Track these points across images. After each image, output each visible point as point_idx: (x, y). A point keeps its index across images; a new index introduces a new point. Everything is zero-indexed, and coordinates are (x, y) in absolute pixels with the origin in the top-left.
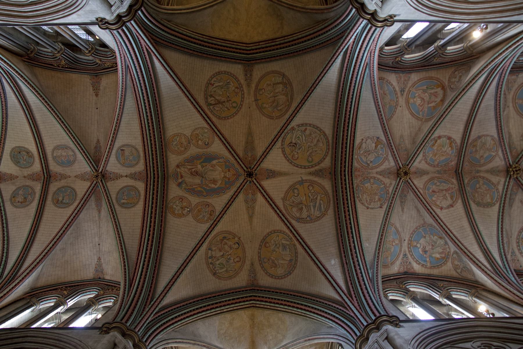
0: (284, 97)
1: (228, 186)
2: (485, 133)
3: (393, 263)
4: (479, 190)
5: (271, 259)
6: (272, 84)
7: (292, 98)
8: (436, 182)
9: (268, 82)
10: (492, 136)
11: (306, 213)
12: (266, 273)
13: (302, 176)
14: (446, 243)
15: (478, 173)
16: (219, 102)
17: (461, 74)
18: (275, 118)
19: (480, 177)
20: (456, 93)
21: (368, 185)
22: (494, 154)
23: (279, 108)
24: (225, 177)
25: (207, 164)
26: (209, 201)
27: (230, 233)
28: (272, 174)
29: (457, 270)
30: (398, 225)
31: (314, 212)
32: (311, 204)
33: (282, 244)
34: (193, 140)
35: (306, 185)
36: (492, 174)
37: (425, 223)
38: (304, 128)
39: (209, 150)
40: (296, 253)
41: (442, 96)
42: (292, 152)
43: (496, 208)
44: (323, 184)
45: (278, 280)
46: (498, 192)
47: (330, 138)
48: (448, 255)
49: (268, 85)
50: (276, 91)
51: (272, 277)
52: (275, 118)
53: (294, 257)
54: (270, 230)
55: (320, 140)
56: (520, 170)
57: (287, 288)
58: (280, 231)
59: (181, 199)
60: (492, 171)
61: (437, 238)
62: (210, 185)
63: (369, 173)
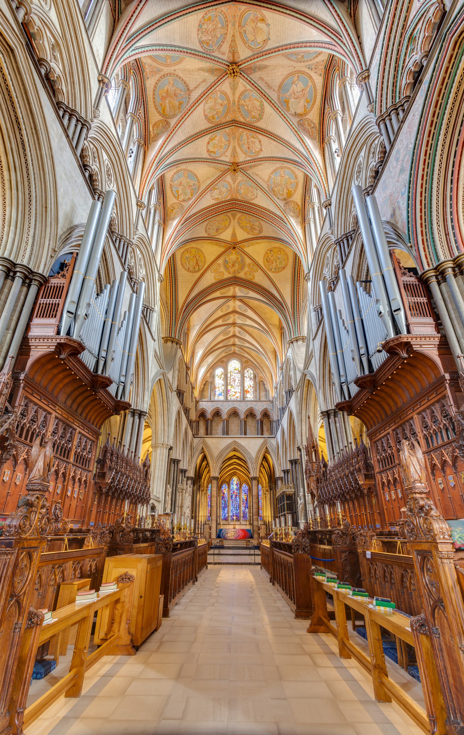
2: (202, 114)
3: (296, 177)
4: (249, 108)
10: (204, 106)
15: (235, 103)
16: (197, 263)
19: (238, 102)
21: (242, 191)
22: (219, 93)
27: (265, 256)
28: (234, 235)
30: (271, 170)
35: (240, 221)
43: (266, 104)
59: (246, 274)
60: (234, 88)
63: (234, 188)
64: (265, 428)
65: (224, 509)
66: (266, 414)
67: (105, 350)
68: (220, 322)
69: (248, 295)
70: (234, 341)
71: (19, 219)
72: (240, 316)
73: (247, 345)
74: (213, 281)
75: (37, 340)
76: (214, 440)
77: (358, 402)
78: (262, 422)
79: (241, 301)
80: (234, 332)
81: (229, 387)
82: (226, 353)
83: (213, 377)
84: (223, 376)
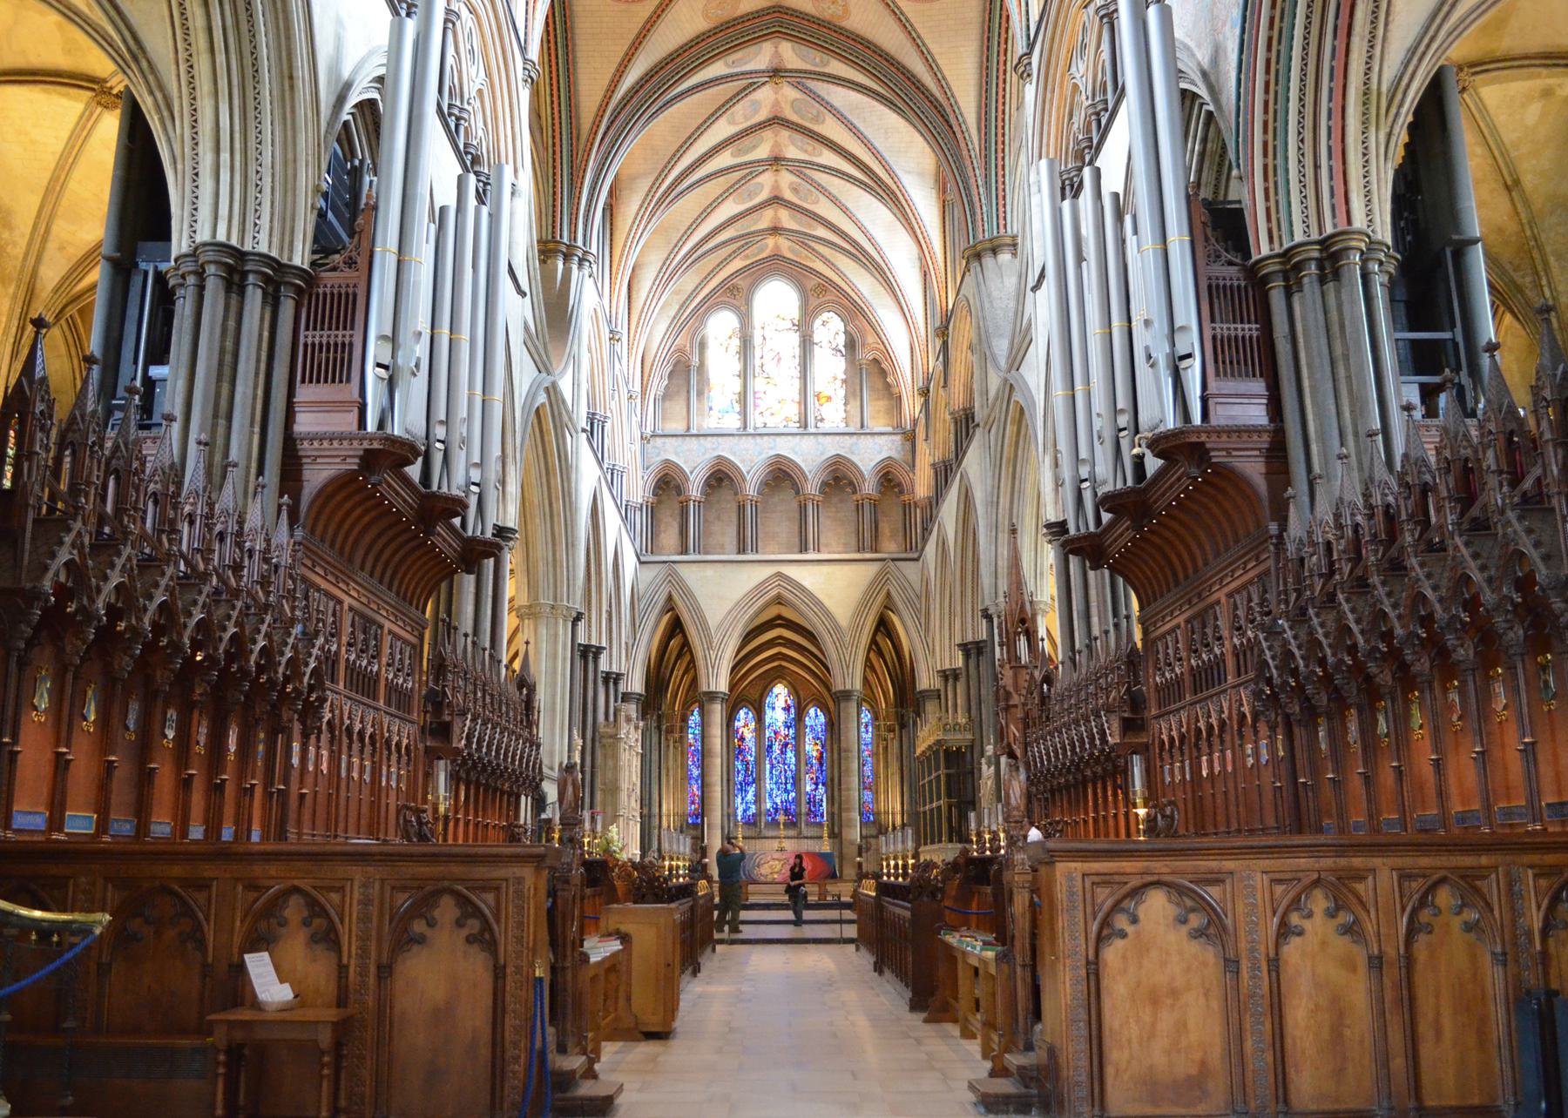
64: (885, 528)
65: (743, 790)
66: (889, 479)
67: (441, 422)
68: (725, 159)
69: (827, 70)
70: (776, 218)
71: (237, 128)
72: (798, 136)
73: (821, 232)
74: (699, 24)
75: (316, 444)
76: (709, 571)
77: (1115, 540)
78: (875, 505)
79: (799, 86)
80: (776, 186)
81: (758, 384)
82: (747, 257)
83: (702, 346)
84: (736, 342)
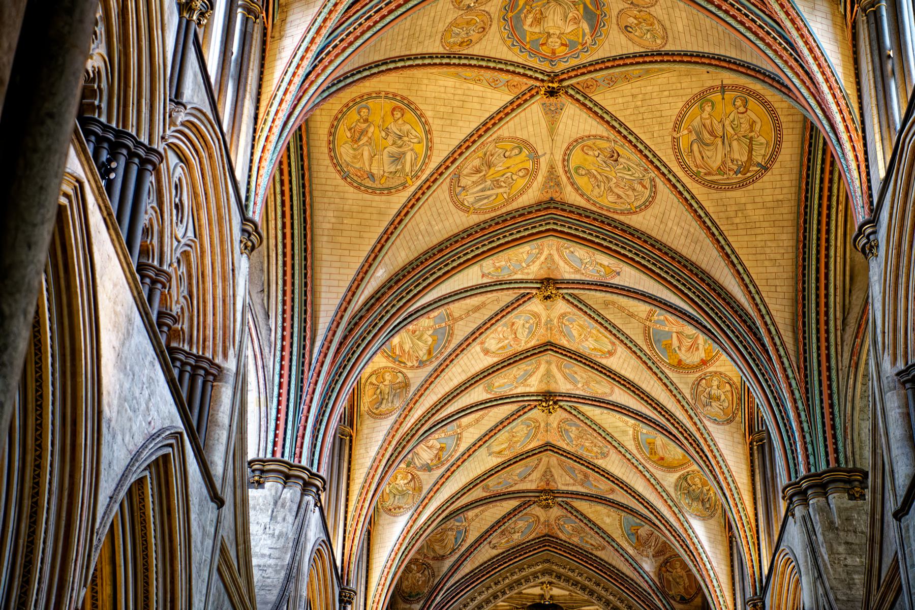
0: (719, 162)
1: (528, 47)
5: (369, 126)
6: (752, 134)
7: (712, 185)
8: (531, 321)
9: (757, 127)
11: (470, 183)
12: (336, 118)
13: (547, 156)
14: (422, 364)
17: (723, 397)
18: (675, 135)
20: (688, 396)
23: (695, 147)
24: (549, 35)
25: (581, 10)
26: (494, 27)
29: (374, 377)
31: (473, 193)
32: (489, 182)
33: (404, 154)
34: (639, 12)
35: (529, 165)
36: (543, 376)
37: (456, 320)
38: (648, 186)
39: (615, 27)
40: (389, 191)
41: (688, 361)
42: (599, 149)
44: (530, 190)
45: (326, 151)
46: (511, 390)
47: (622, 218)
48: (401, 362)
49: (752, 124)
50: (735, 144)
51: (330, 134)
52: (675, 135)
53: (379, 186)
54: (430, 120)
55: (622, 201)
56: (550, 412)
57: (315, 175)
58: (429, 148)
61: (430, 343)
62: (531, 16)
